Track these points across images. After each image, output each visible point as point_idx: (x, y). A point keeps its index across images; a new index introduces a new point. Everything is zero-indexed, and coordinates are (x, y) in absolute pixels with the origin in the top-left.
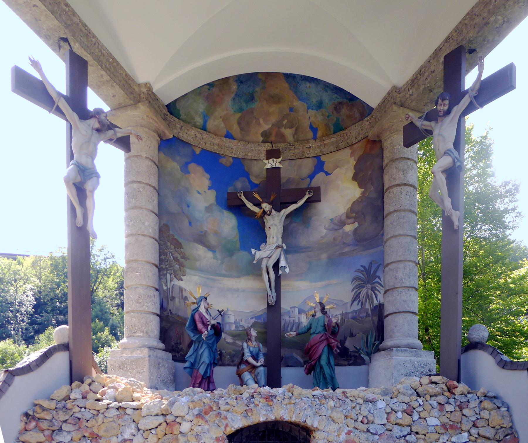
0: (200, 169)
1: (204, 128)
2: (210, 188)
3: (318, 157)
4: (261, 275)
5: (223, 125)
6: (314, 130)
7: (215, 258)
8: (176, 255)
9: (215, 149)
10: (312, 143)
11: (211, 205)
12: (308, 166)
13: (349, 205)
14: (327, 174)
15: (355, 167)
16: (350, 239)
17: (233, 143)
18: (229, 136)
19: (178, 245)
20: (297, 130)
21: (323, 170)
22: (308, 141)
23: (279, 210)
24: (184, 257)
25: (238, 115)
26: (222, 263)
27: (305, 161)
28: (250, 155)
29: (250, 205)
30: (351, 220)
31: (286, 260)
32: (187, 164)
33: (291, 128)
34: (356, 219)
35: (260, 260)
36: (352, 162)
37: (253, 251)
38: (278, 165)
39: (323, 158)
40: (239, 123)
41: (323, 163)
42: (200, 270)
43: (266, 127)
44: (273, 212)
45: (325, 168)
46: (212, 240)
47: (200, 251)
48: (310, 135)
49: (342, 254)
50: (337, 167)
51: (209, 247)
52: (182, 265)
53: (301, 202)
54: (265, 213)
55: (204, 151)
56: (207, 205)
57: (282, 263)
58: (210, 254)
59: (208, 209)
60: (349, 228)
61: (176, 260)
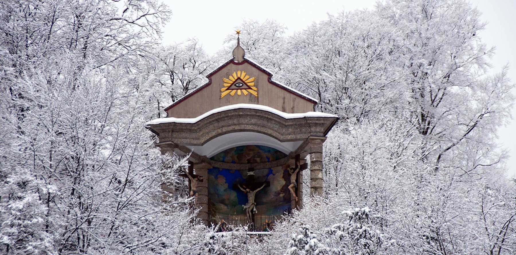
0: (222, 176)
1: (223, 161)
2: (226, 183)
3: (270, 168)
4: (246, 214)
5: (231, 159)
6: (268, 158)
7: (228, 208)
8: (213, 208)
9: (228, 168)
10: (267, 163)
11: (226, 189)
12: (266, 171)
13: (282, 187)
14: (274, 175)
15: (283, 173)
16: (282, 199)
17: (235, 165)
18: (233, 162)
19: (214, 205)
20: (261, 158)
21: (272, 174)
22: (266, 162)
23: (253, 191)
24: (216, 209)
25: (237, 155)
26: (231, 210)
27: (265, 169)
28: (242, 168)
29: (242, 189)
30: (282, 193)
31: (256, 209)
32: (217, 175)
33: (259, 158)
34: (284, 192)
35: (246, 209)
36: (282, 171)
37: (243, 206)
38: (253, 174)
39: (272, 169)
40: (237, 157)
41: (272, 171)
42: (222, 213)
43: (249, 158)
44: (251, 191)
45: (273, 172)
46: (227, 202)
47: (222, 206)
48: (267, 160)
49: (279, 205)
50: (277, 172)
51: (226, 205)
52: (215, 212)
53: (262, 188)
54: (247, 192)
55: (223, 169)
56: (224, 189)
57: (255, 210)
58: (226, 207)
59: (225, 190)
60: (281, 195)
61: (213, 210)
